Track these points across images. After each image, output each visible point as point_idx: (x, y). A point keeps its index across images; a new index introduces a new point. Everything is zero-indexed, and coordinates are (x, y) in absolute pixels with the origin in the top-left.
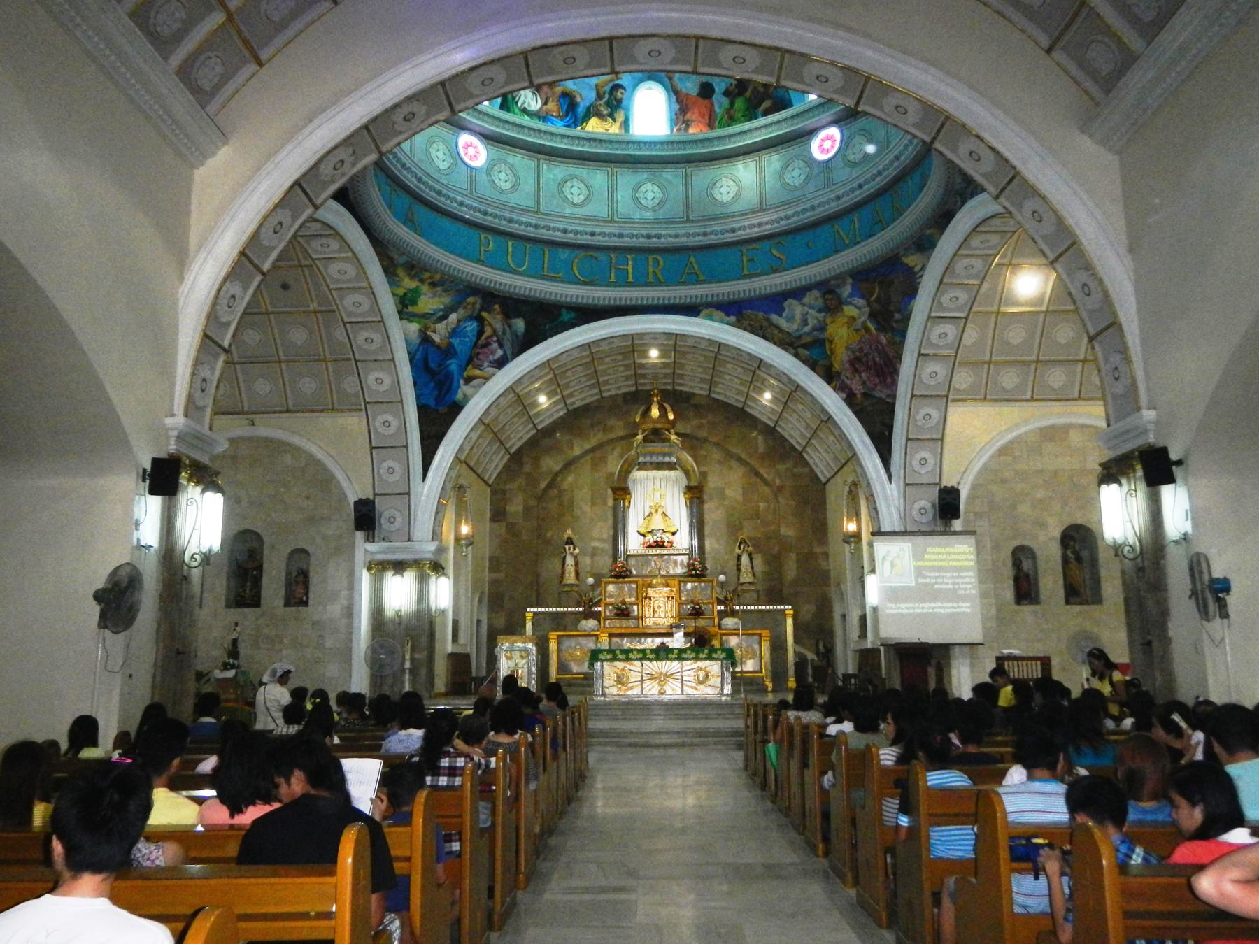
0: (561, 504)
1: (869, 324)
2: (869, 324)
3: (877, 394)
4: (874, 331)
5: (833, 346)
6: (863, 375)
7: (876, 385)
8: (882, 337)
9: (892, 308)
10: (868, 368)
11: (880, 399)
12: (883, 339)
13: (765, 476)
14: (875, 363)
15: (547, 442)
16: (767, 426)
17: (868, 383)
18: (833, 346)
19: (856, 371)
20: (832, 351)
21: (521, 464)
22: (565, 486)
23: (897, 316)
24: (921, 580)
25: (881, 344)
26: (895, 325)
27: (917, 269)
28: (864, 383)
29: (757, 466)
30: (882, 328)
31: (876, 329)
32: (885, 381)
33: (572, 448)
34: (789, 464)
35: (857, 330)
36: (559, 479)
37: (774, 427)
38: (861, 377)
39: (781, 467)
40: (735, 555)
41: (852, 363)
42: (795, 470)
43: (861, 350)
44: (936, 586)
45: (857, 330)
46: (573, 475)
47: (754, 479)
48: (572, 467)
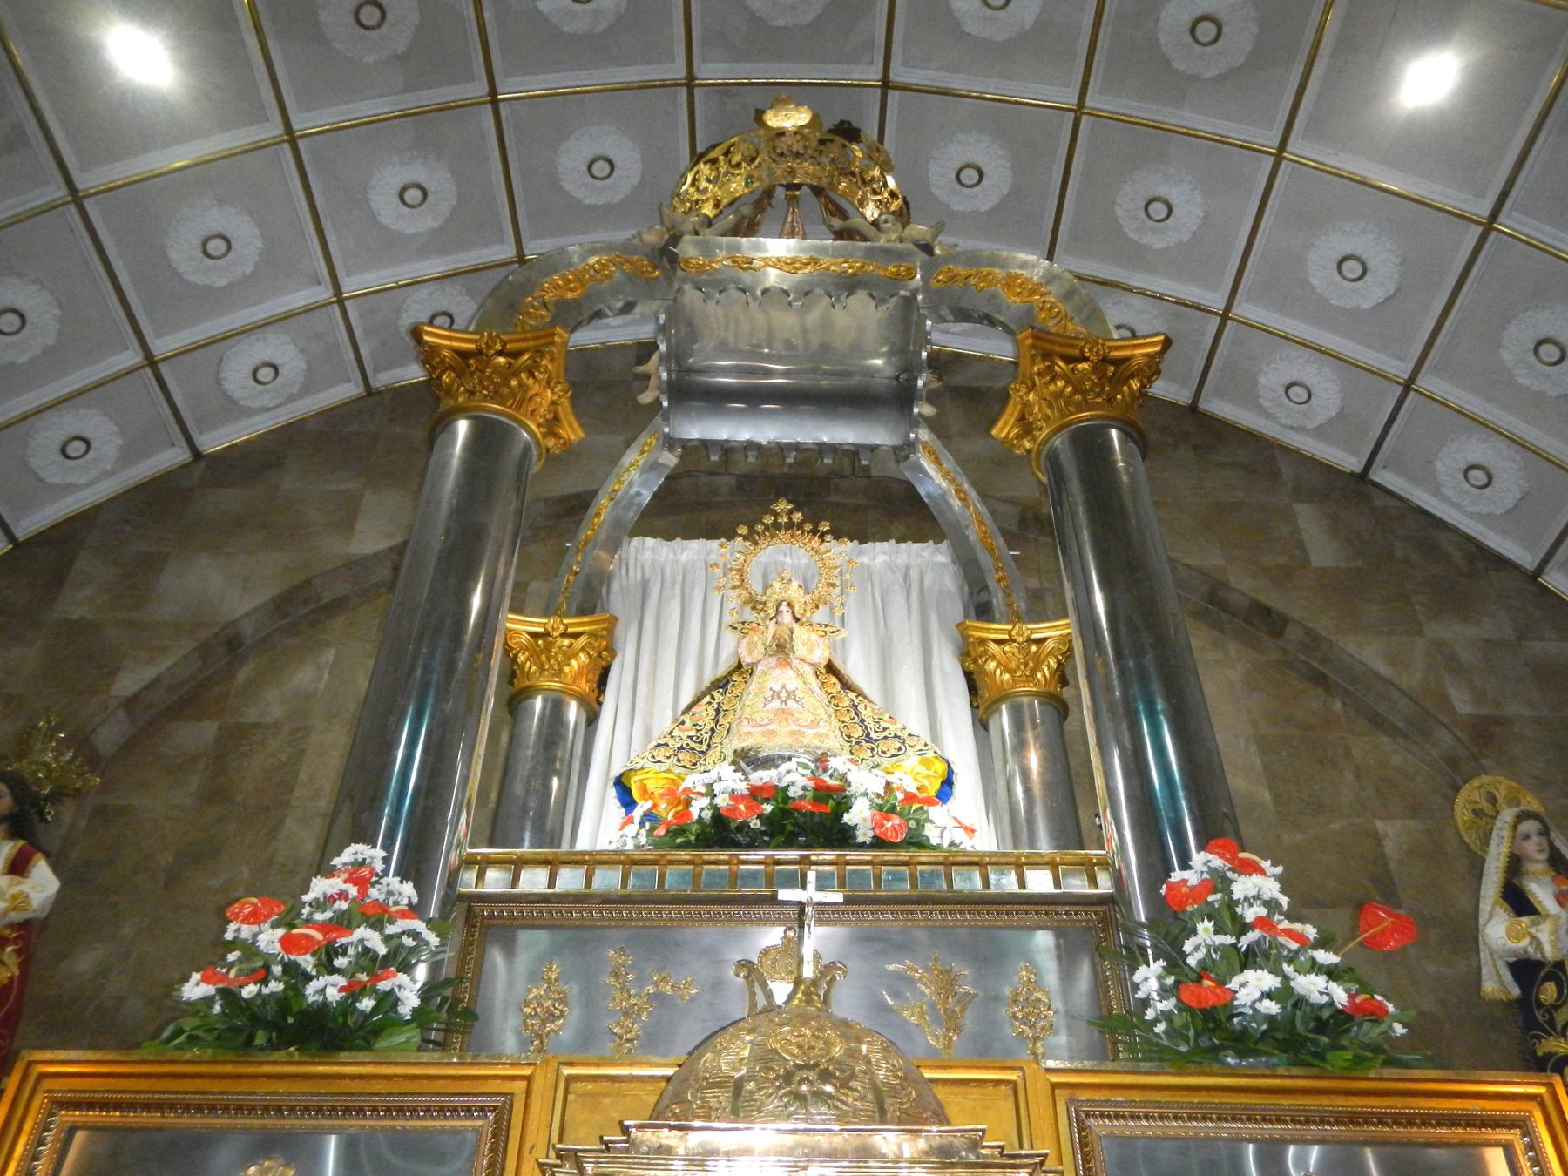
0: (215, 794)
13: (1383, 669)
15: (231, 498)
16: (1329, 471)
21: (57, 579)
22: (272, 706)
29: (1323, 625)
33: (346, 521)
34: (1494, 625)
36: (244, 674)
37: (1363, 476)
39: (1460, 635)
40: (1496, 984)
42: (1535, 647)
46: (330, 655)
47: (1313, 701)
48: (340, 622)
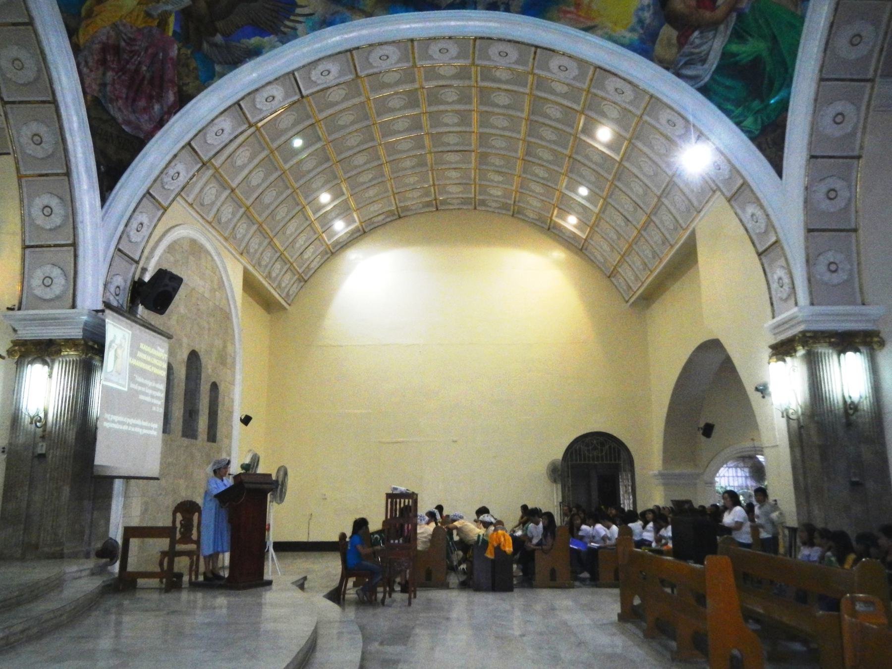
1: (172, 20)
2: (172, 20)
3: (114, 111)
4: (170, 34)
5: (97, 9)
6: (110, 74)
7: (118, 98)
8: (176, 47)
9: (220, 24)
10: (122, 70)
11: (114, 119)
12: (174, 52)
14: (137, 71)
17: (109, 88)
18: (97, 9)
19: (103, 62)
20: (90, 14)
23: (219, 38)
24: (132, 386)
25: (166, 53)
26: (205, 46)
27: (298, 11)
28: (103, 85)
30: (183, 37)
31: (174, 32)
32: (134, 100)
35: (148, 15)
38: (104, 74)
41: (105, 48)
43: (131, 41)
44: (142, 397)
45: (148, 15)
